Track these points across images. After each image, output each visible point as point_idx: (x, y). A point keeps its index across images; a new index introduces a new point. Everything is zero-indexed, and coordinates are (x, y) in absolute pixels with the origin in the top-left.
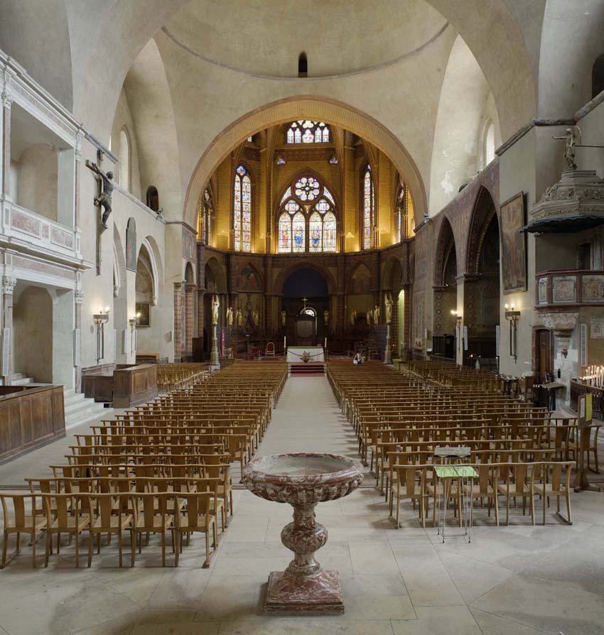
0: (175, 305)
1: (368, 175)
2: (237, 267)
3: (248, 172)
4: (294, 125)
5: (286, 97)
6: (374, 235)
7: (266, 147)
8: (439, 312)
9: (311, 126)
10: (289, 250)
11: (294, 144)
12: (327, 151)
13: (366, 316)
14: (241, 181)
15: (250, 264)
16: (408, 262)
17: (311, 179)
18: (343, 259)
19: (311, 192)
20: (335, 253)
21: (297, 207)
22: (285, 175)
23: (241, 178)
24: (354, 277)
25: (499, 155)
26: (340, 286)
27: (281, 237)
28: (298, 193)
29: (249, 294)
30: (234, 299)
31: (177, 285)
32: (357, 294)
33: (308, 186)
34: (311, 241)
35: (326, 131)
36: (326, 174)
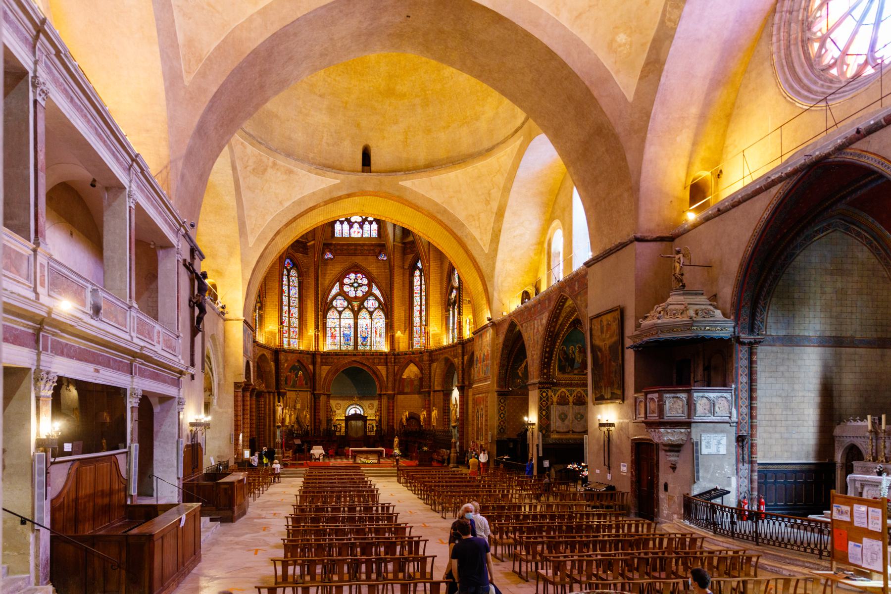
1: (417, 273)
2: (286, 365)
3: (295, 265)
5: (349, 192)
7: (314, 240)
8: (502, 415)
9: (360, 219)
10: (336, 348)
11: (342, 238)
12: (377, 247)
13: (420, 418)
14: (289, 276)
16: (463, 363)
17: (359, 275)
18: (394, 359)
19: (359, 288)
21: (346, 304)
22: (333, 271)
23: (289, 271)
25: (588, 267)
26: (390, 385)
27: (329, 334)
28: (346, 289)
32: (407, 394)
33: (357, 282)
34: (359, 339)
35: (375, 226)
36: (373, 270)
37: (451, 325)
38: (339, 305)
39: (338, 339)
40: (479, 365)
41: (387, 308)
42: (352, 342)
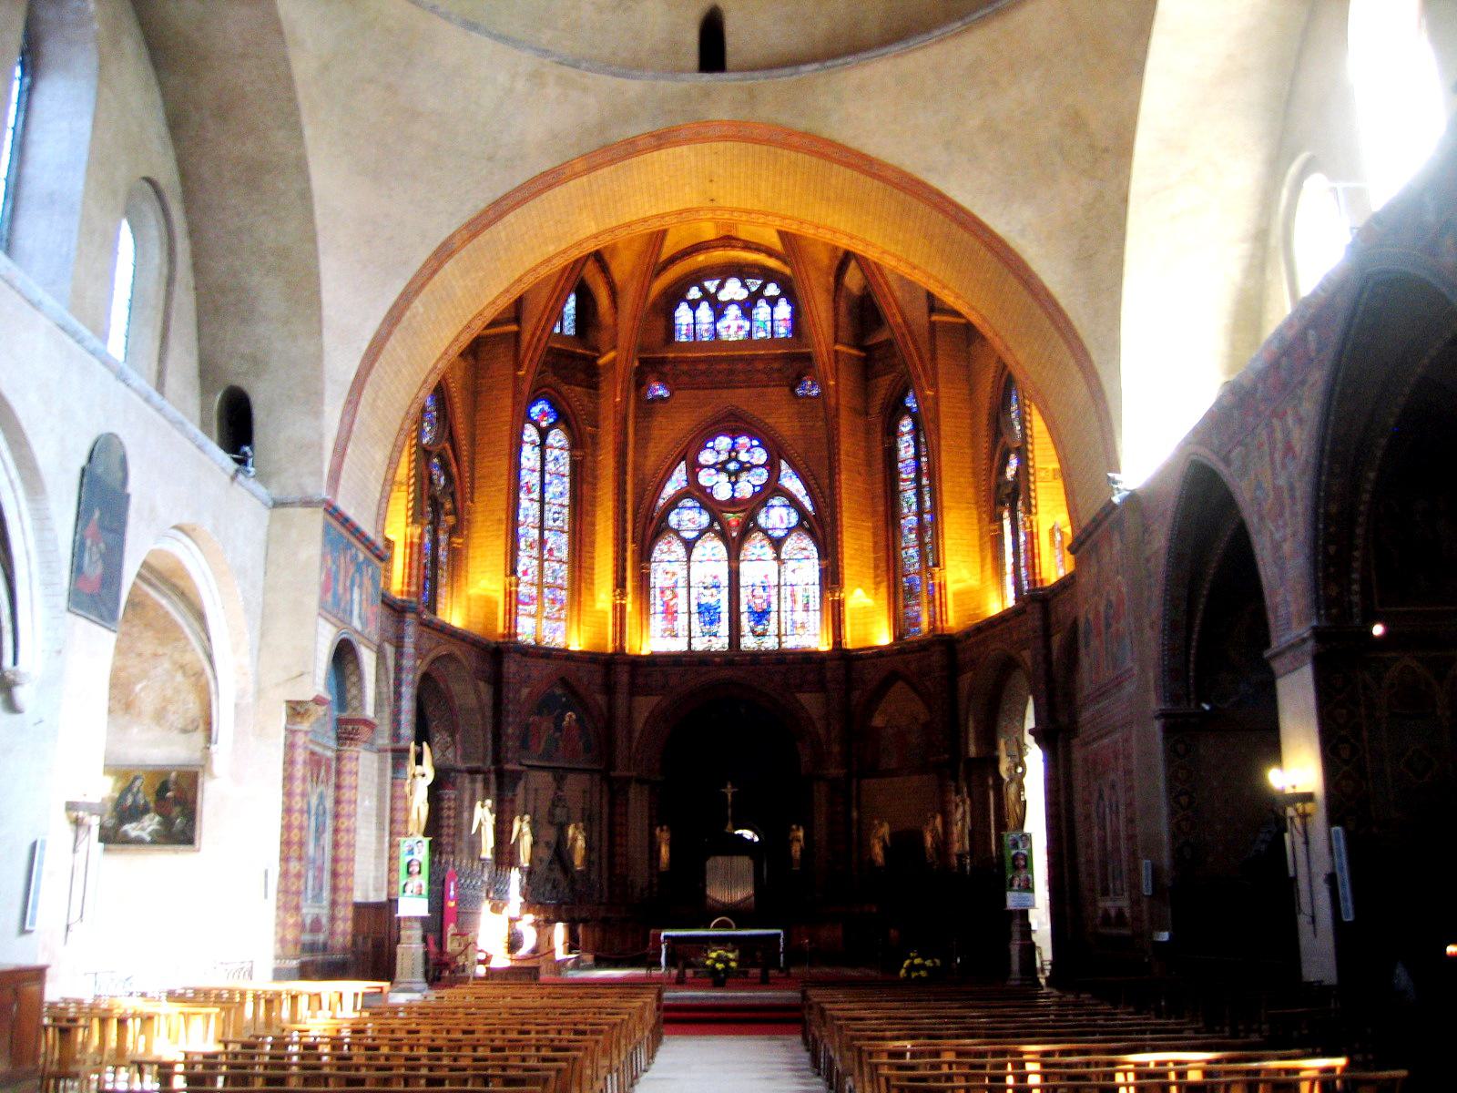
0: (288, 778)
1: (906, 425)
2: (525, 691)
4: (694, 293)
5: (661, 125)
6: (936, 594)
7: (615, 347)
8: (1184, 799)
9: (742, 294)
10: (679, 645)
11: (696, 344)
14: (543, 446)
15: (564, 682)
17: (743, 440)
19: (744, 476)
20: (817, 653)
22: (669, 430)
23: (543, 434)
24: (878, 721)
26: (836, 749)
27: (658, 606)
28: (705, 478)
29: (560, 775)
30: (515, 785)
31: (296, 710)
33: (736, 459)
34: (744, 619)
35: (784, 310)
37: (1009, 559)
38: (686, 525)
39: (682, 620)
40: (1095, 643)
41: (822, 527)
42: (723, 628)
